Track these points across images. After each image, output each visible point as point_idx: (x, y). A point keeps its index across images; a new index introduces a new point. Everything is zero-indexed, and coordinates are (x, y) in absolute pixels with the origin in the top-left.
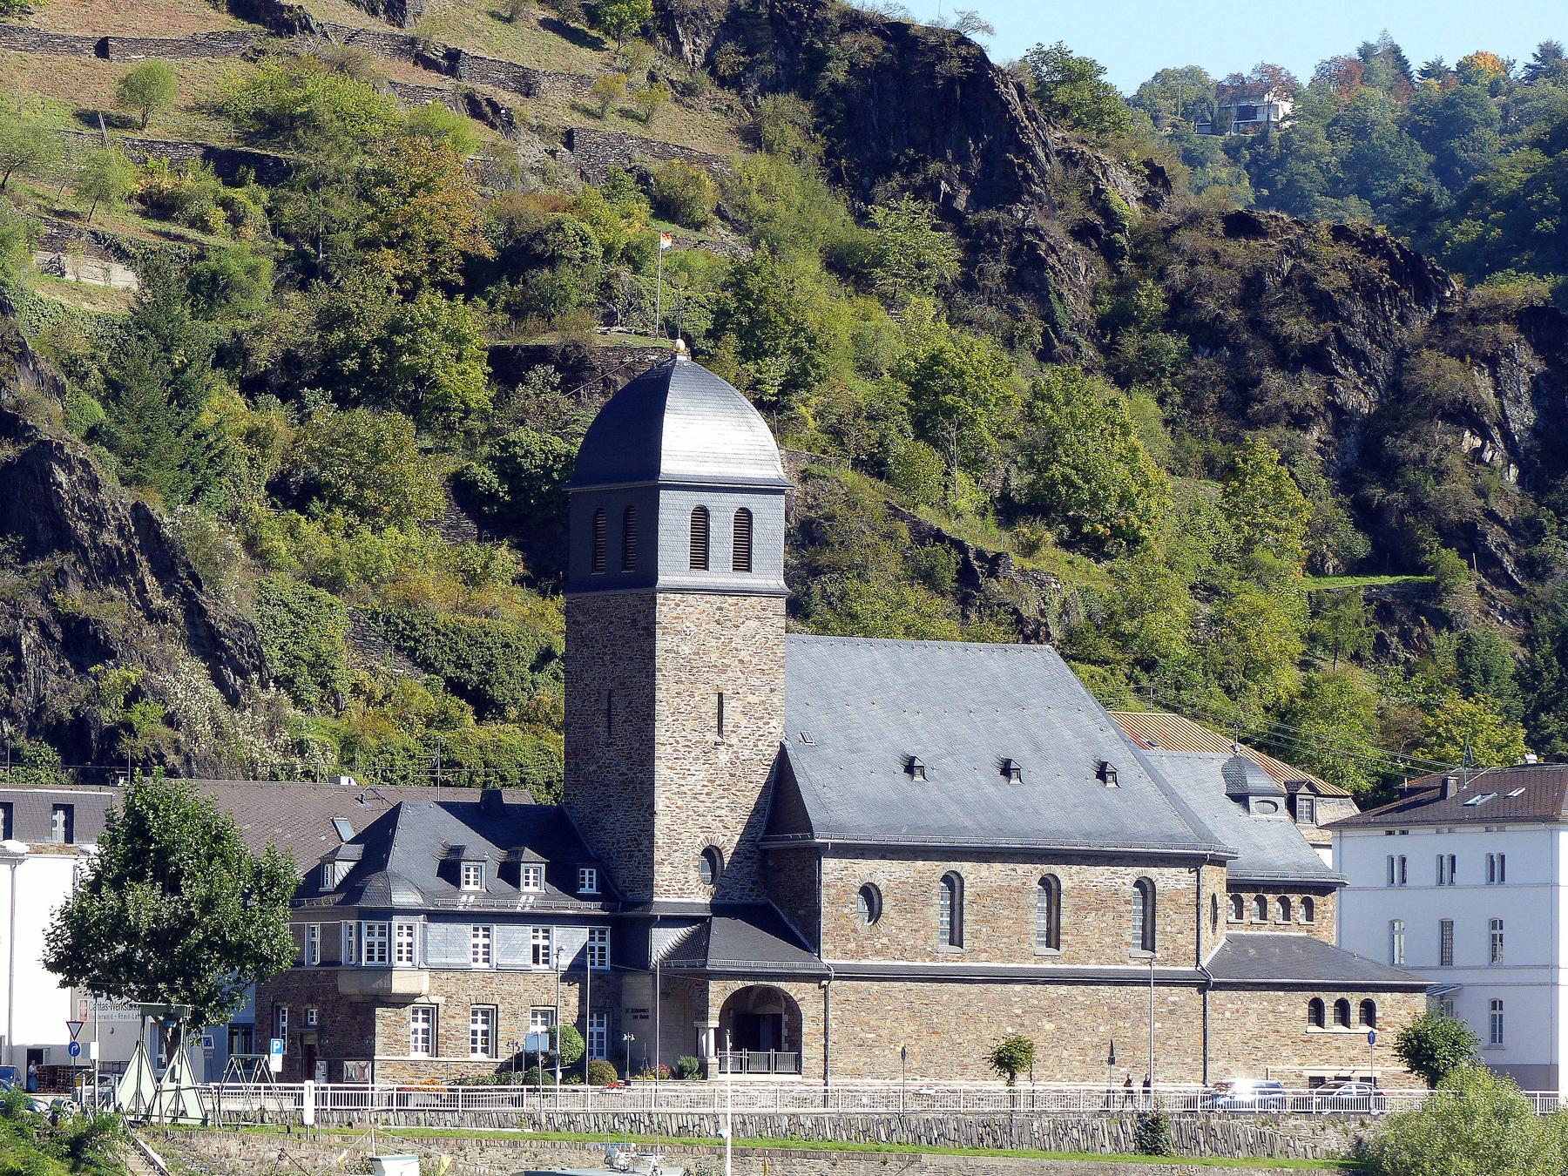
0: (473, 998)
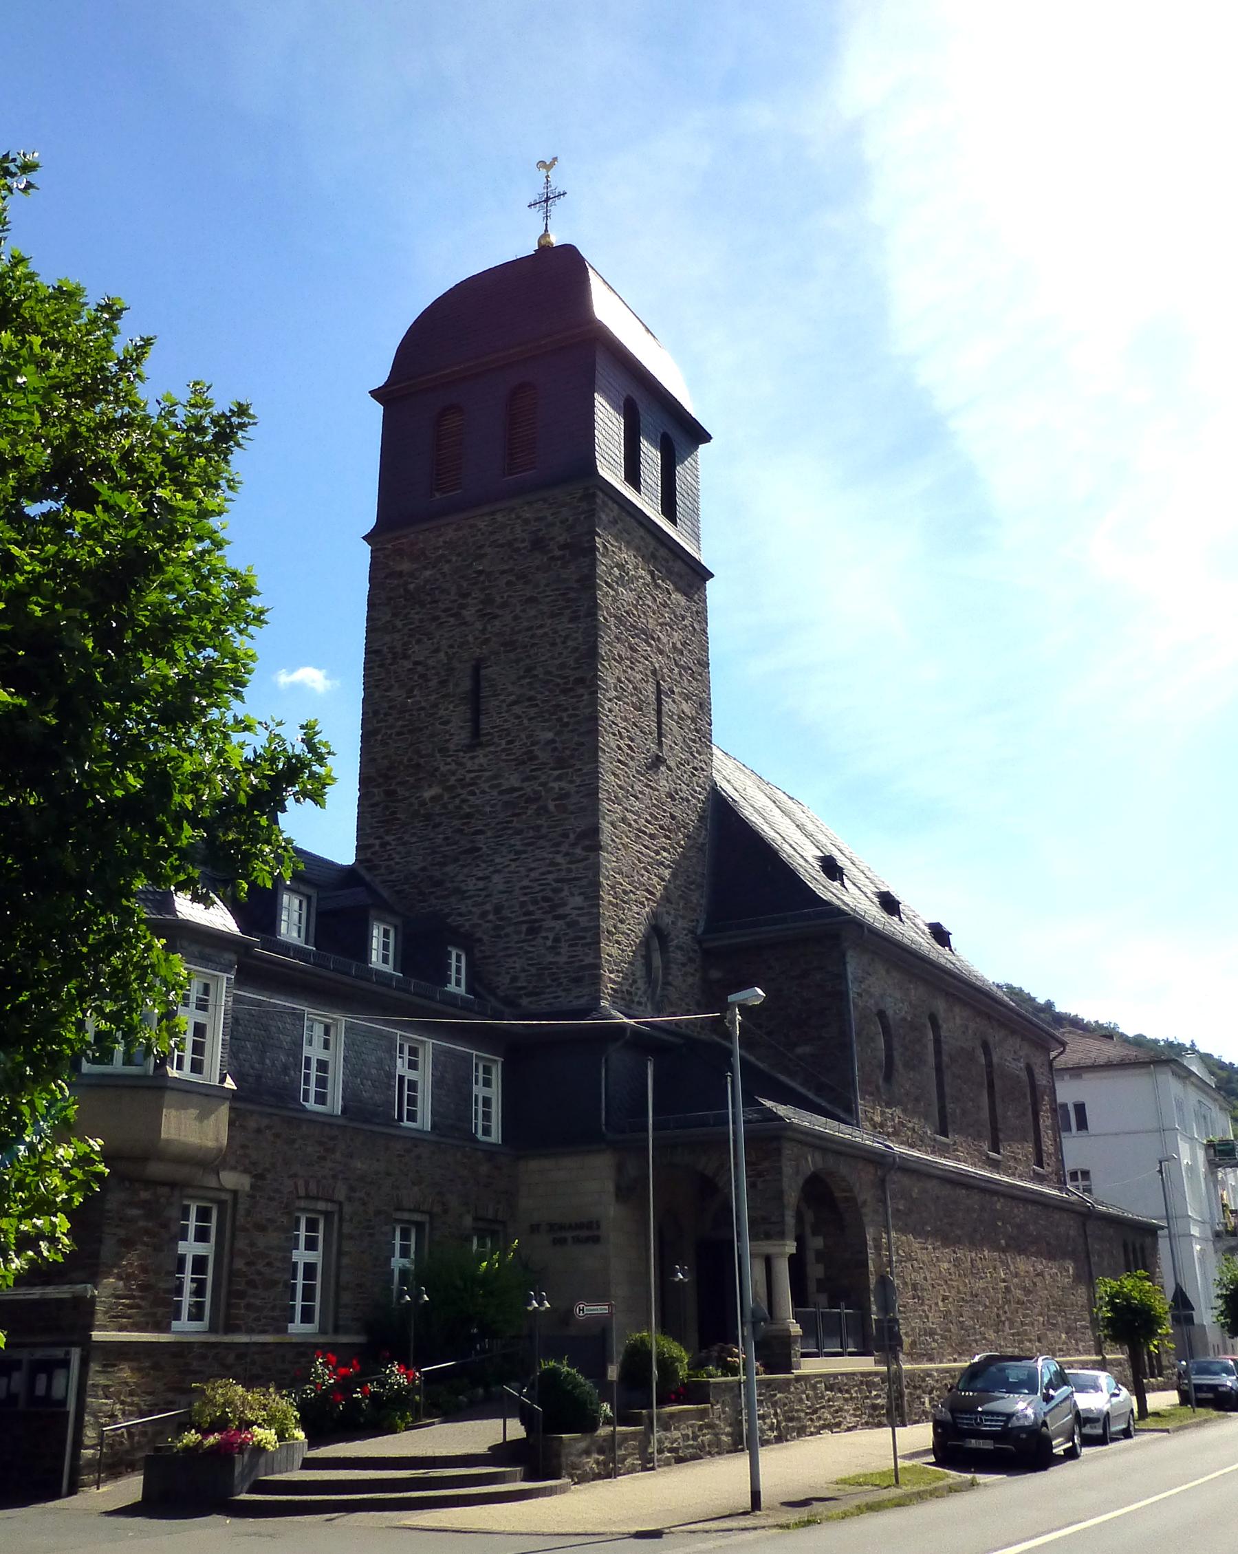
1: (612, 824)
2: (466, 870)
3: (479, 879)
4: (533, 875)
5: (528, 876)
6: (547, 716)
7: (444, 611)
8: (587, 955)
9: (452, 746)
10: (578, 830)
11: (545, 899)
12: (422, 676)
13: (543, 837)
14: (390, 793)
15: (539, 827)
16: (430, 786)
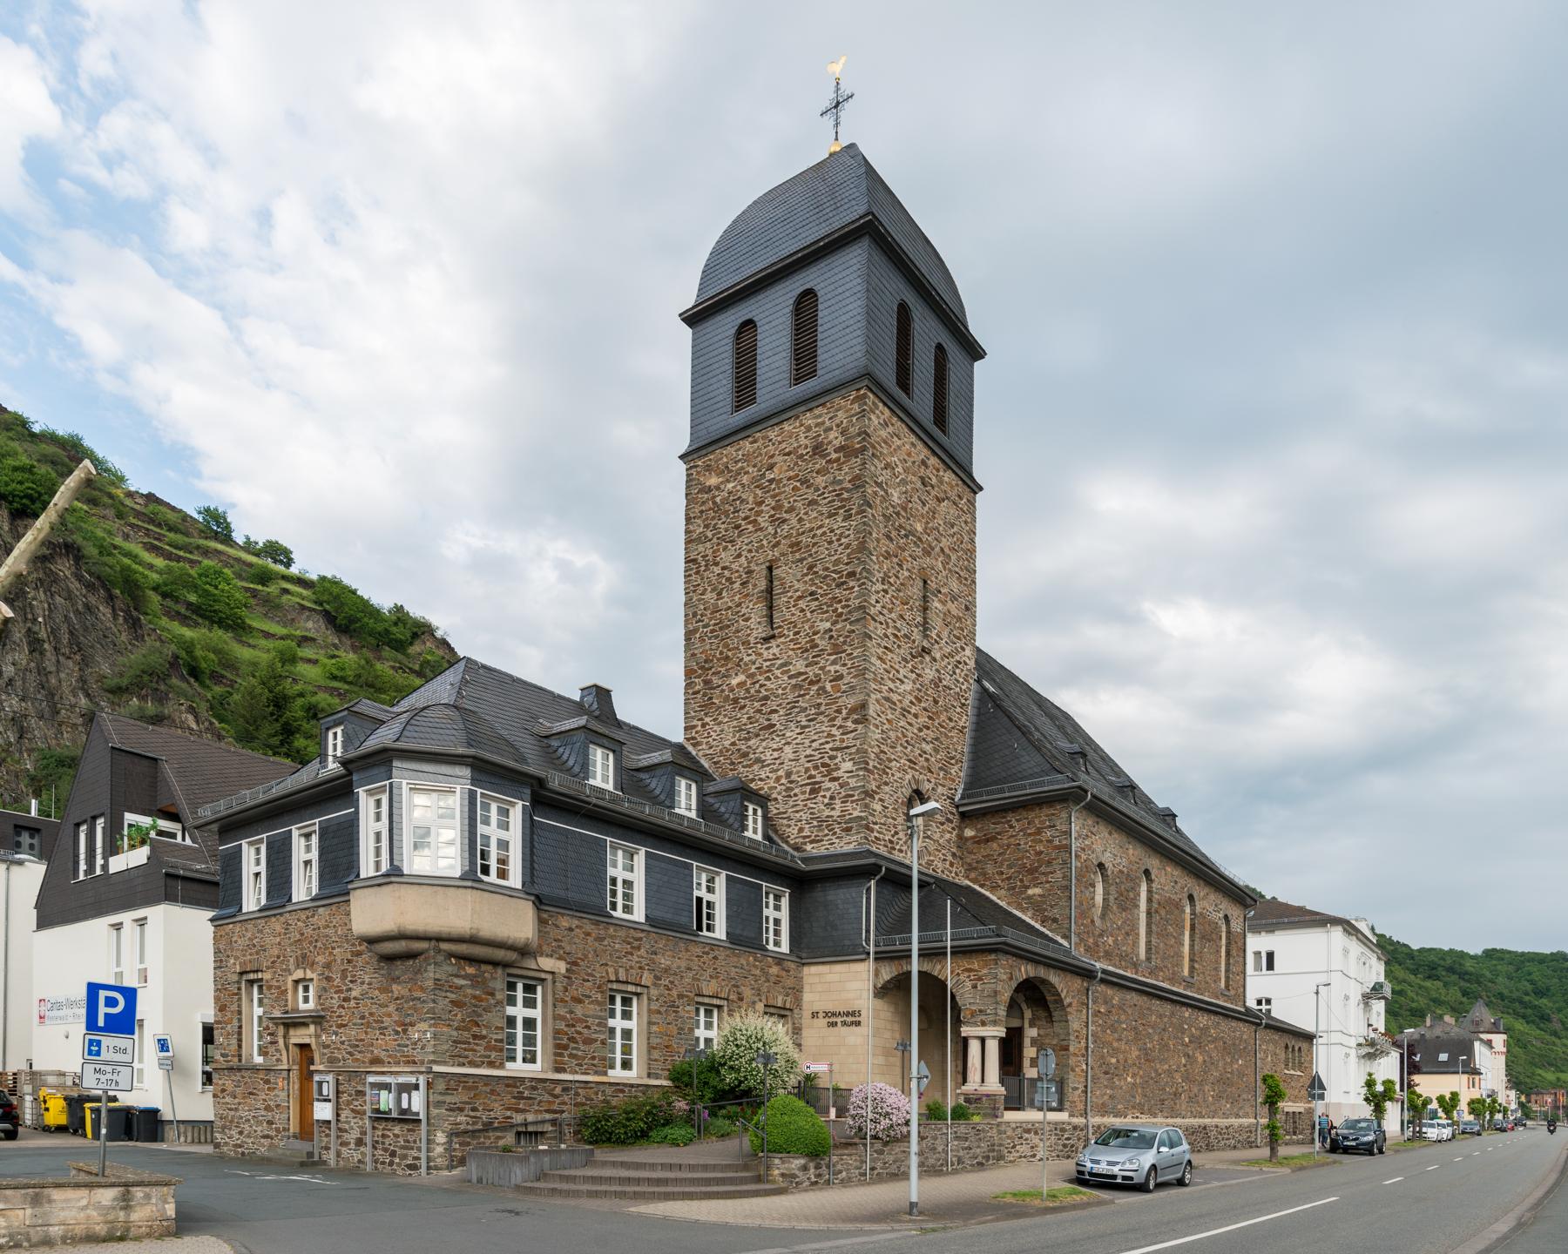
0: (611, 970)
1: (877, 701)
2: (764, 744)
3: (774, 750)
4: (815, 745)
5: (810, 746)
6: (825, 607)
7: (744, 519)
8: (854, 809)
9: (752, 640)
10: (849, 706)
11: (824, 765)
12: (728, 579)
13: (822, 713)
14: (706, 682)
15: (820, 704)
16: (736, 674)
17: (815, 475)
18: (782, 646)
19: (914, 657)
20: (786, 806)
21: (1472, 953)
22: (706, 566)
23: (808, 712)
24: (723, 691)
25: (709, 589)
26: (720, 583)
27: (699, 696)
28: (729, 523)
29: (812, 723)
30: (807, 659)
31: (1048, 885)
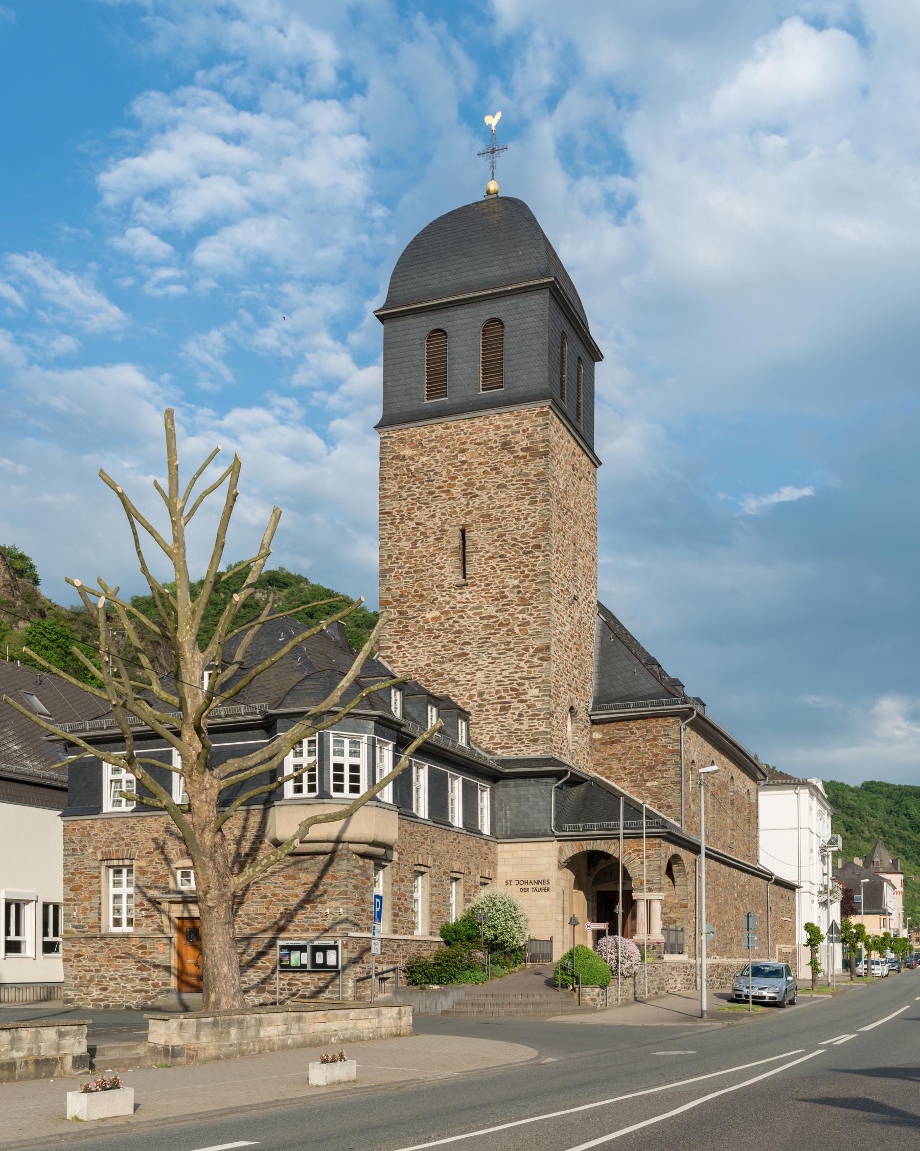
2: (458, 668)
3: (467, 674)
4: (504, 673)
5: (500, 674)
9: (446, 585)
10: (536, 647)
11: (513, 689)
13: (511, 649)
15: (509, 643)
16: (431, 610)
17: (503, 465)
18: (474, 593)
19: (570, 605)
20: (479, 719)
21: (852, 786)
22: (401, 519)
23: (498, 647)
24: (418, 622)
25: (405, 538)
26: (415, 535)
27: (394, 623)
28: (424, 489)
29: (502, 656)
30: (497, 606)
31: (663, 780)
